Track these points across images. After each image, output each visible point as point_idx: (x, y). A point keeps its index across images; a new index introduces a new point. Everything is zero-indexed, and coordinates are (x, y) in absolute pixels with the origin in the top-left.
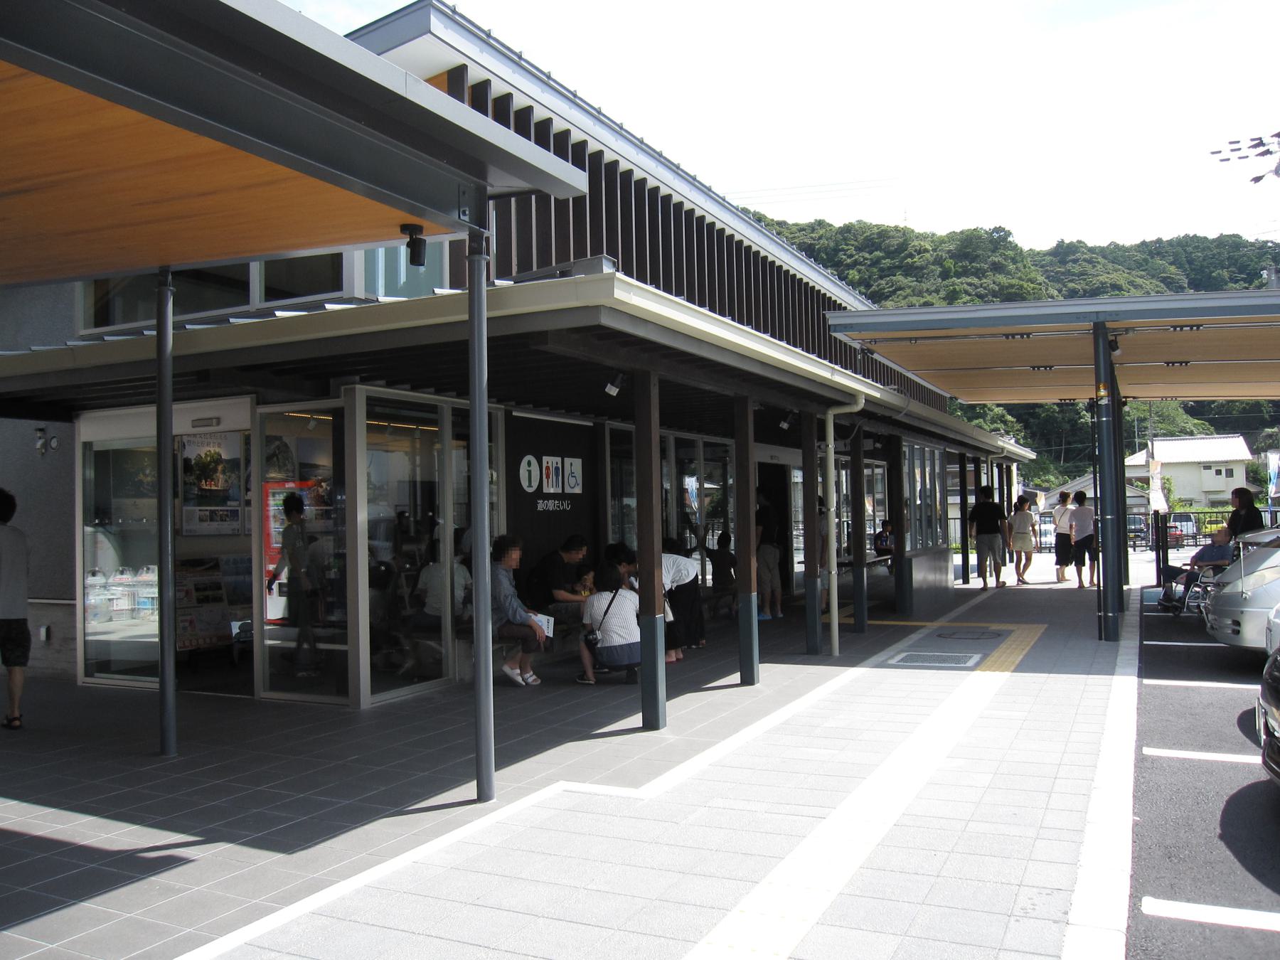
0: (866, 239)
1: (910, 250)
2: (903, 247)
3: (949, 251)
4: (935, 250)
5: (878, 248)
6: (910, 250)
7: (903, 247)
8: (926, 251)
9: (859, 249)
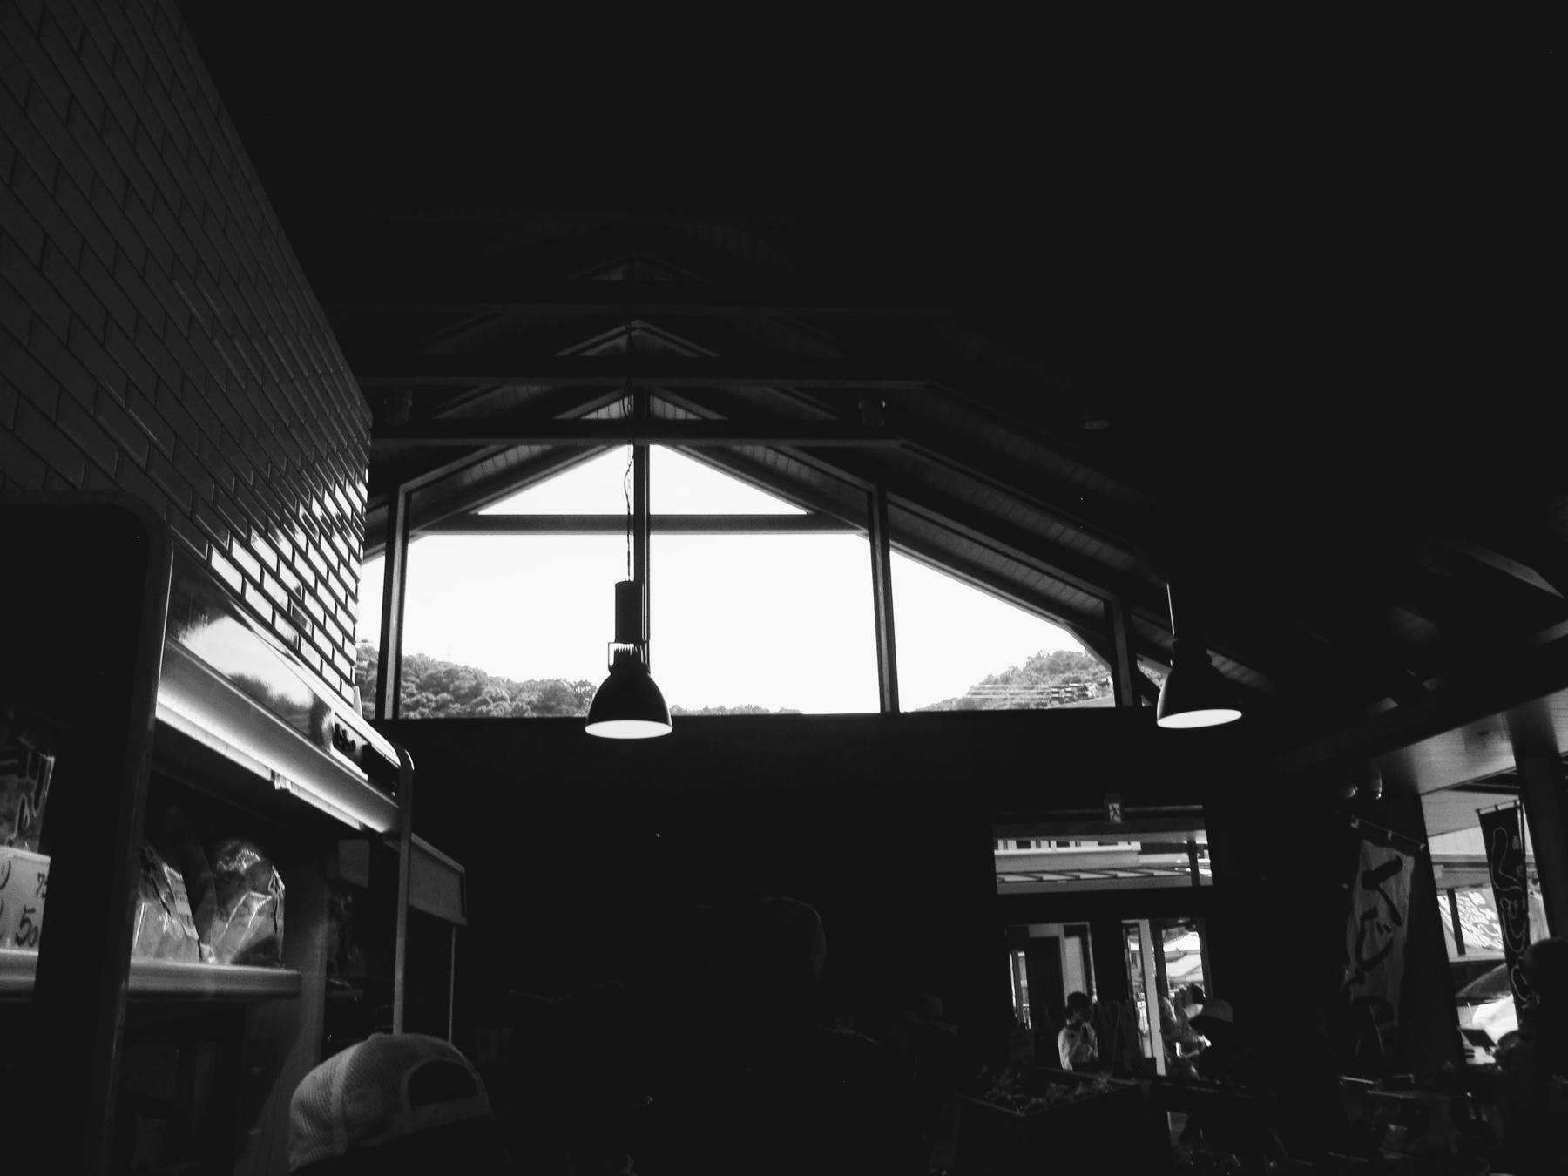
0: (431, 677)
1: (484, 695)
2: (476, 691)
3: (529, 703)
4: (512, 699)
5: (445, 689)
6: (484, 695)
7: (476, 691)
8: (503, 699)
9: (421, 688)
